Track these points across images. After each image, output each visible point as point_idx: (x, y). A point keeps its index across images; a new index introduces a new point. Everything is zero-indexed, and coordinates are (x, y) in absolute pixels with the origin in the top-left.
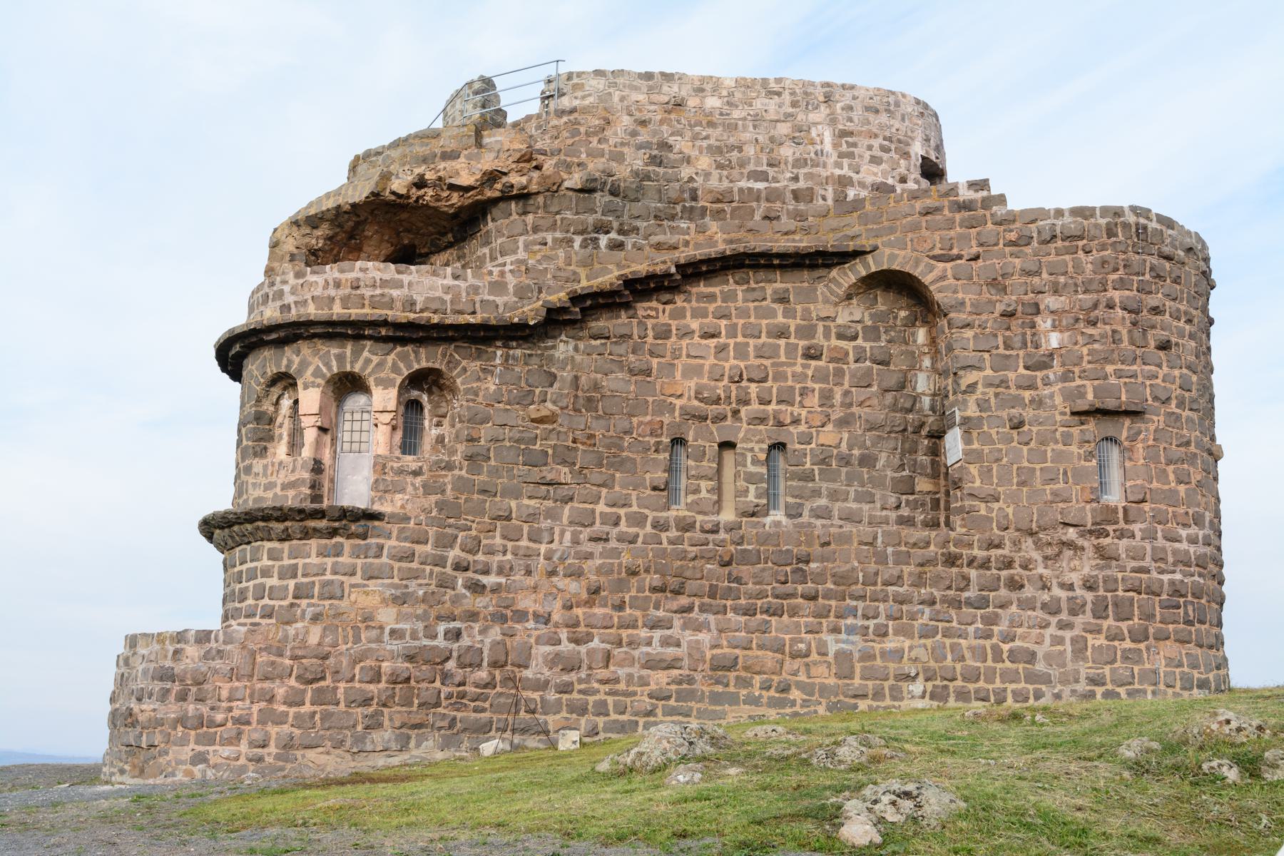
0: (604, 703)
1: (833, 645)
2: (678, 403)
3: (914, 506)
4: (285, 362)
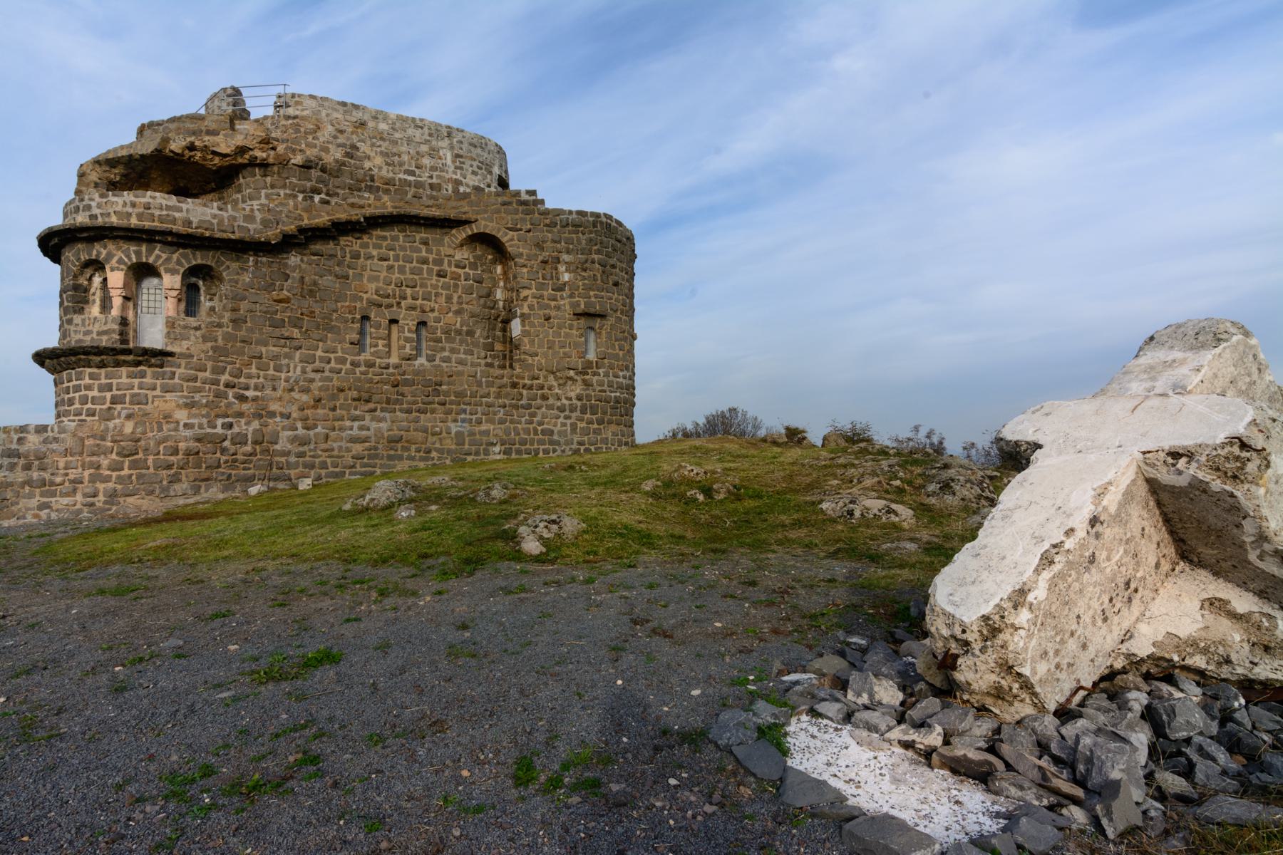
0: (325, 462)
1: (454, 428)
2: (365, 296)
3: (493, 357)
4: (95, 252)
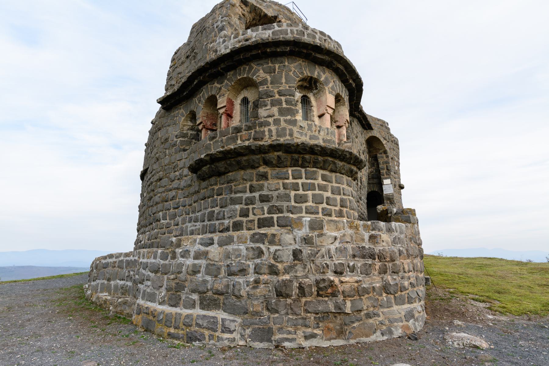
4: (316, 73)
